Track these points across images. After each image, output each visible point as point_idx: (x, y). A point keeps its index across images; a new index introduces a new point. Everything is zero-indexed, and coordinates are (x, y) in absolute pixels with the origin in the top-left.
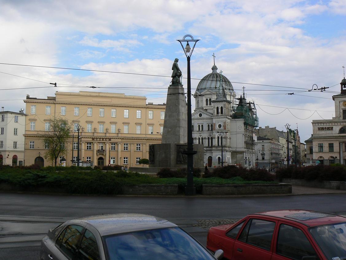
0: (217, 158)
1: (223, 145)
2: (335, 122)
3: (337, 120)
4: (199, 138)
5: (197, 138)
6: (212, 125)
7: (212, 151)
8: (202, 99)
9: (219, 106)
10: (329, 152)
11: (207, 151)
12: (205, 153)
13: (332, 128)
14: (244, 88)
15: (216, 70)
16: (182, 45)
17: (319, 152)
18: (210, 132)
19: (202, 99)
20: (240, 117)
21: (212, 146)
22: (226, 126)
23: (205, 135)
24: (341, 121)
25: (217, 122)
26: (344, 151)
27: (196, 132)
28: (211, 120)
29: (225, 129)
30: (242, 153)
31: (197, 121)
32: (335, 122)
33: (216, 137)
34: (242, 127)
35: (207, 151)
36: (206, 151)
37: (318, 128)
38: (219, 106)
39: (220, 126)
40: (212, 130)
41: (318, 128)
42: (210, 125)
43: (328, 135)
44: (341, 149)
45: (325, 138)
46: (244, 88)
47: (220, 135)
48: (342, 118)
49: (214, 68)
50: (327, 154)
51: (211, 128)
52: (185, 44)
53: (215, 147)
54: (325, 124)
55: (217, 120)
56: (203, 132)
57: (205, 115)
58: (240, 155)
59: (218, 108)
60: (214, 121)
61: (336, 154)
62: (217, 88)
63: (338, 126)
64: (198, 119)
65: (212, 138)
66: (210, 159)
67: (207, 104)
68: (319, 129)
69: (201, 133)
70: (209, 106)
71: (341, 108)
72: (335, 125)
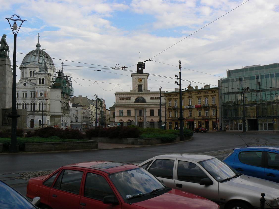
0: (38, 120)
1: (43, 110)
2: (132, 94)
3: (133, 92)
4: (23, 104)
5: (22, 104)
6: (34, 93)
7: (34, 115)
8: (26, 71)
9: (41, 77)
10: (128, 116)
11: (30, 115)
12: (28, 117)
13: (130, 99)
14: (62, 64)
15: (39, 47)
16: (10, 23)
17: (120, 116)
18: (33, 99)
19: (26, 71)
20: (58, 87)
21: (34, 111)
22: (47, 94)
23: (29, 101)
24: (136, 93)
25: (39, 90)
26: (138, 116)
28: (34, 89)
29: (45, 96)
30: (59, 116)
31: (21, 89)
32: (132, 94)
33: (38, 103)
34: (60, 96)
35: (29, 114)
36: (28, 115)
37: (120, 98)
38: (41, 77)
39: (41, 94)
40: (34, 97)
41: (120, 98)
42: (33, 93)
43: (126, 104)
44: (136, 114)
45: (125, 106)
46: (62, 64)
47: (41, 102)
48: (137, 91)
49: (38, 46)
50: (126, 118)
51: (34, 95)
52: (12, 22)
53: (36, 111)
54: (125, 95)
55: (39, 89)
56: (26, 99)
57: (28, 84)
58: (58, 118)
59: (40, 79)
60: (37, 90)
61: (132, 118)
62: (39, 62)
63: (134, 97)
64: (22, 88)
65: (34, 104)
66: (32, 122)
67: (31, 76)
68: (120, 99)
69: (26, 99)
70: (32, 77)
71: (137, 83)
72: (132, 96)
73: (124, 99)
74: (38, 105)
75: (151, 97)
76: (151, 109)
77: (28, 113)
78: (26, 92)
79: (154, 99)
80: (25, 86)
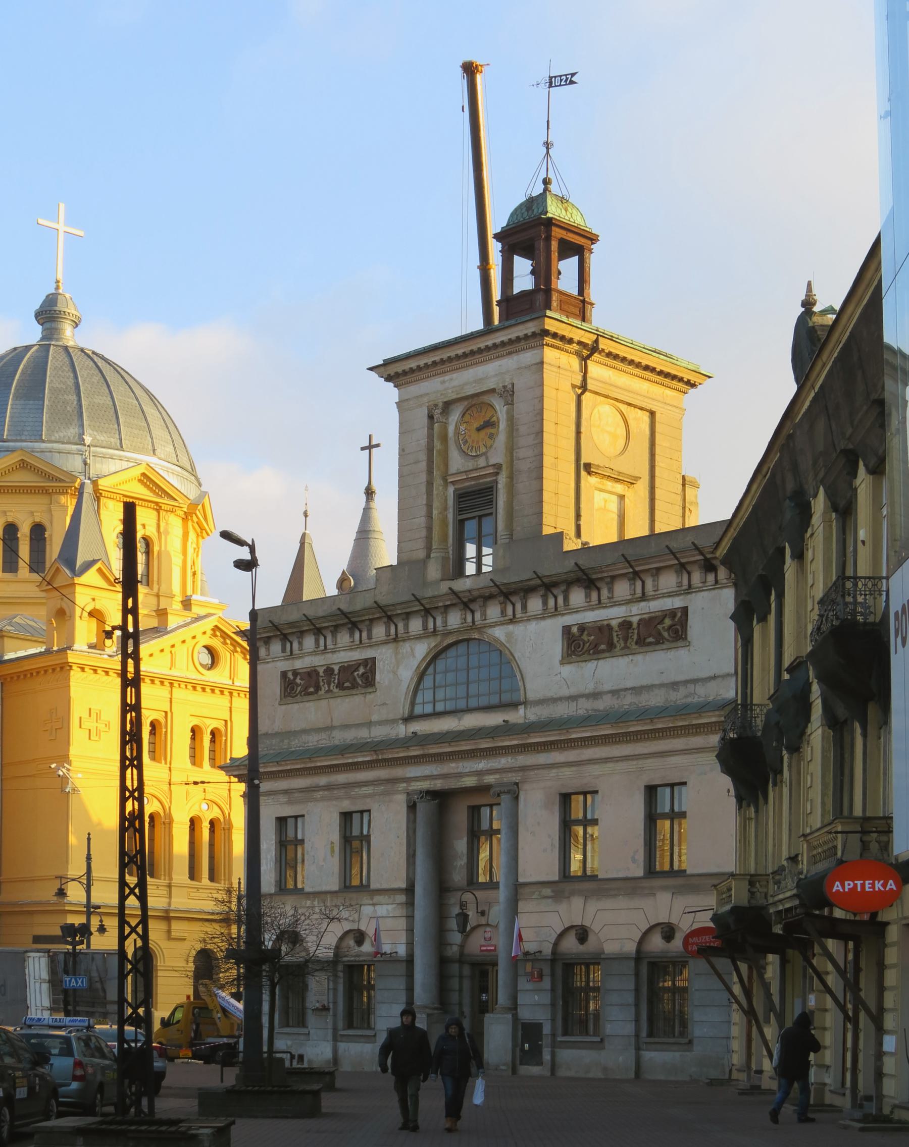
37: (284, 674)
41: (284, 674)
73: (318, 688)
75: (582, 628)
76: (569, 779)
79: (611, 646)
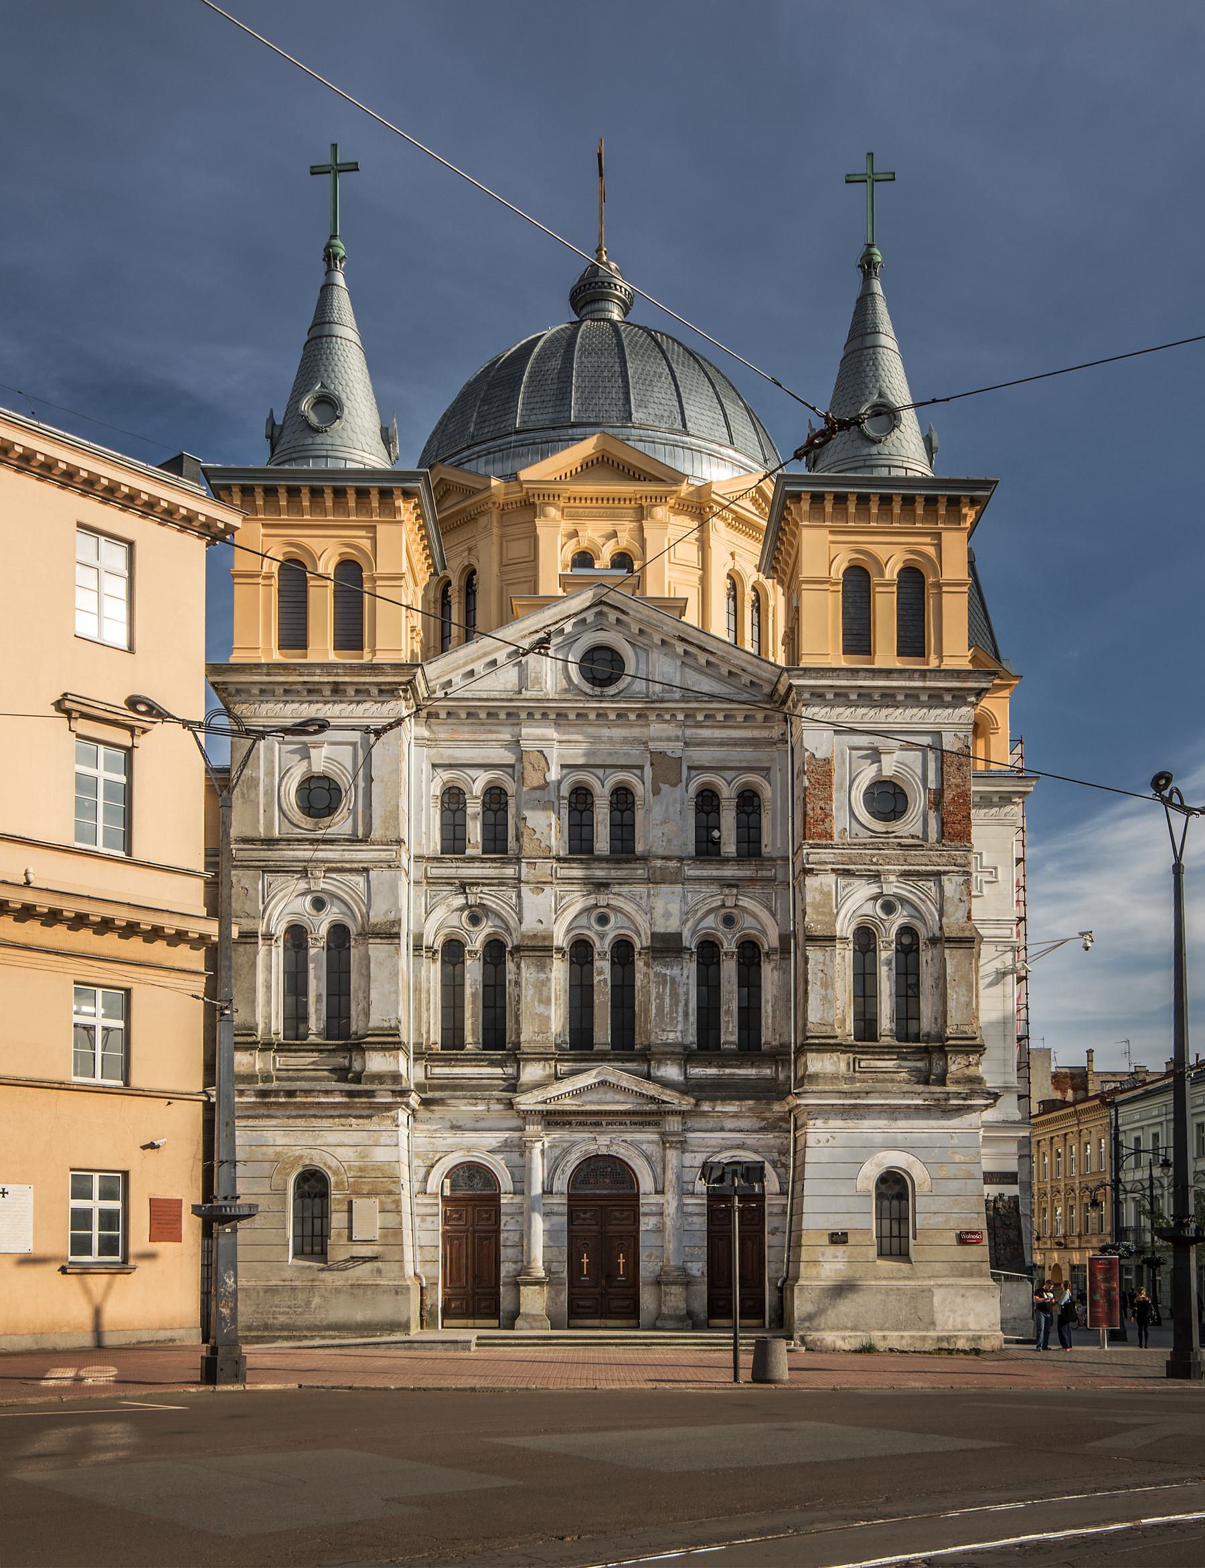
0: (869, 1173)
18: (729, 872)
27: (545, 868)
33: (844, 927)
36: (687, 1103)
47: (889, 908)
74: (843, 959)
77: (672, 1072)
78: (622, 776)
80: (612, 690)
